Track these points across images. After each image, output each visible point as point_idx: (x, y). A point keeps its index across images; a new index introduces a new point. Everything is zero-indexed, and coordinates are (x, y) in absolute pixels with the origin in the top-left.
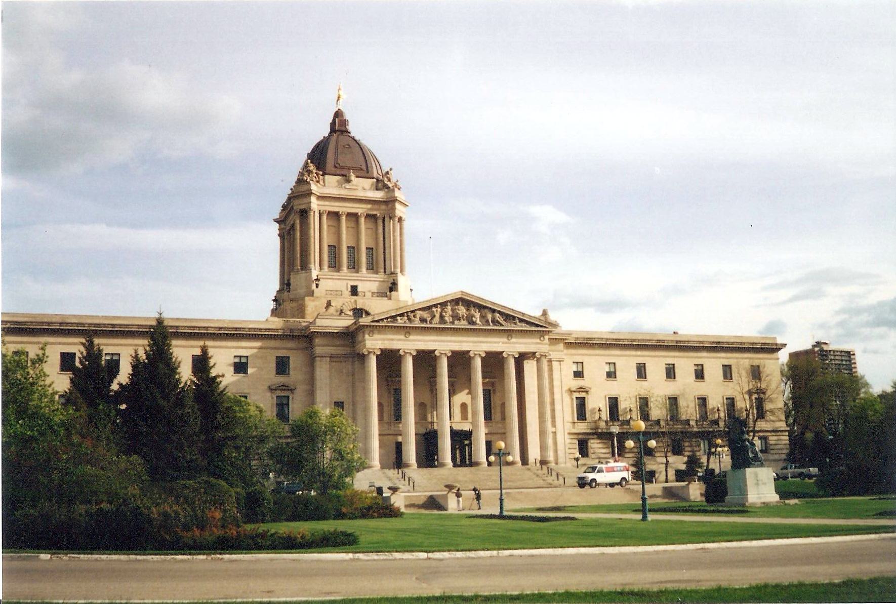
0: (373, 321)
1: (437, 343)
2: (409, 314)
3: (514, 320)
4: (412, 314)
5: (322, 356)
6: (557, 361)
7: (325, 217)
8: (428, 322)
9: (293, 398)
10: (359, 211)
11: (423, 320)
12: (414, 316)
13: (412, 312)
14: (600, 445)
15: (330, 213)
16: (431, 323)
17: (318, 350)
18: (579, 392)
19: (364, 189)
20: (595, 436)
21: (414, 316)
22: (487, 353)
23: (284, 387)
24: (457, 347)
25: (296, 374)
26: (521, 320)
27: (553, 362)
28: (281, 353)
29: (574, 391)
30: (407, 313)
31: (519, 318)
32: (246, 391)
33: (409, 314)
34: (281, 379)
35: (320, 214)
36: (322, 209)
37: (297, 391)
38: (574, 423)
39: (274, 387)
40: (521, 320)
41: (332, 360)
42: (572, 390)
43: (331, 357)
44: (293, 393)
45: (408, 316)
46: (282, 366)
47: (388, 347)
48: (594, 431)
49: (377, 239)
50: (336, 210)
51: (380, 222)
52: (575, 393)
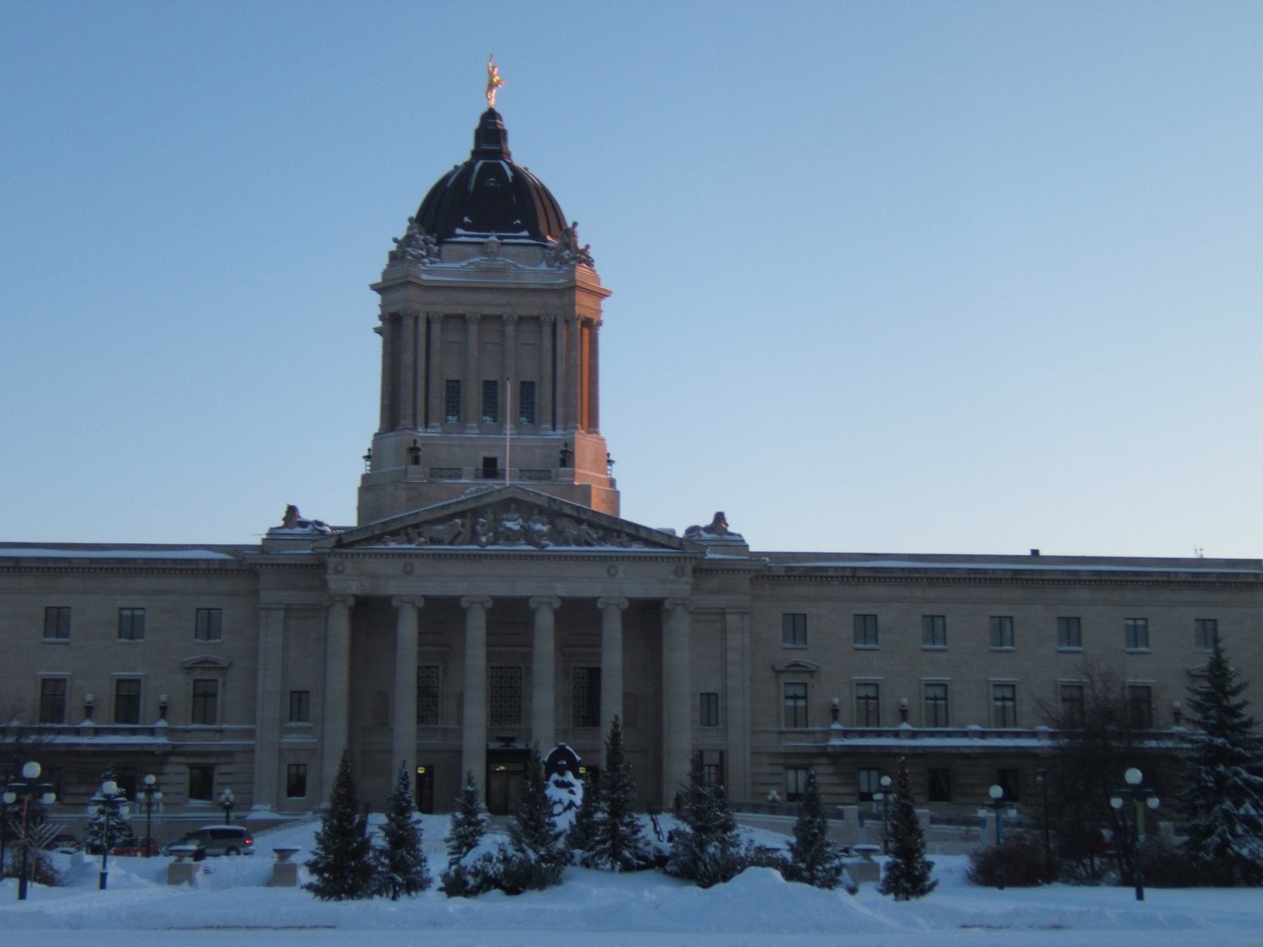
2: (409, 530)
3: (619, 537)
5: (270, 609)
7: (436, 328)
9: (224, 684)
13: (416, 526)
15: (447, 318)
17: (267, 596)
18: (794, 672)
20: (824, 761)
23: (206, 664)
27: (729, 618)
29: (781, 672)
30: (405, 528)
31: (628, 535)
33: (409, 530)
35: (428, 322)
42: (778, 669)
45: (407, 534)
46: (208, 625)
50: (460, 311)
51: (547, 330)
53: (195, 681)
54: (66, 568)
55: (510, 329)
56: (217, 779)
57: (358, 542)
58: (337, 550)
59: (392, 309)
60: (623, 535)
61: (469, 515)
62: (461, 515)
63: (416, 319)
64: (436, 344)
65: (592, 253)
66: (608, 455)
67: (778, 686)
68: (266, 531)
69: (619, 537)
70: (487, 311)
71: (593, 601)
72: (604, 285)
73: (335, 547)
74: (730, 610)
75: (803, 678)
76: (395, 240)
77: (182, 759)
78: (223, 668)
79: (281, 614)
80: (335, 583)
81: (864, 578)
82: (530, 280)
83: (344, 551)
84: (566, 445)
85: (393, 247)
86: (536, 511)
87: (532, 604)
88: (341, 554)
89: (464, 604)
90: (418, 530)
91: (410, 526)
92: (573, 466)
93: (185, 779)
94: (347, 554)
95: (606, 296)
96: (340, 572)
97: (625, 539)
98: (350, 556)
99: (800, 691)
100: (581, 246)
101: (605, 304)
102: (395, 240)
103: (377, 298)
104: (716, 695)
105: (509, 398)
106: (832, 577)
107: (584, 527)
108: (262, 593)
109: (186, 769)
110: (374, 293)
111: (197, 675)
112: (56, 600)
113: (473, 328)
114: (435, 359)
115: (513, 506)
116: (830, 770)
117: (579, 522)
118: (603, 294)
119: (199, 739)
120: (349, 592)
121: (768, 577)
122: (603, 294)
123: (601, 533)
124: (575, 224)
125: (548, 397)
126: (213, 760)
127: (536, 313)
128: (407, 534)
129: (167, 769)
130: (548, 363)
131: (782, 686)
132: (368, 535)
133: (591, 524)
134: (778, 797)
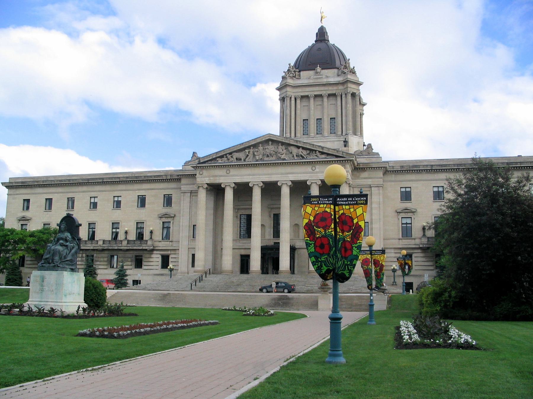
0: (199, 164)
1: (251, 177)
4: (230, 155)
5: (186, 192)
6: (376, 187)
7: (298, 101)
8: (243, 161)
10: (323, 93)
11: (238, 159)
12: (232, 157)
13: (230, 154)
14: (424, 259)
15: (302, 97)
17: (184, 188)
19: (327, 77)
20: (419, 251)
22: (292, 182)
23: (166, 215)
24: (267, 179)
26: (322, 153)
28: (167, 192)
29: (400, 212)
30: (226, 155)
31: (319, 152)
32: (143, 219)
34: (167, 210)
36: (297, 94)
38: (399, 239)
40: (322, 153)
41: (193, 194)
43: (191, 193)
44: (173, 219)
45: (227, 157)
46: (168, 201)
47: (213, 182)
48: (417, 246)
49: (337, 111)
50: (306, 94)
51: (339, 99)
52: (401, 214)
53: (163, 222)
54: (119, 181)
55: (325, 99)
56: (170, 260)
57: (207, 161)
59: (282, 96)
60: (317, 152)
61: (252, 147)
62: (249, 147)
63: (291, 98)
64: (298, 106)
65: (356, 69)
66: (364, 143)
67: (399, 219)
68: (185, 162)
69: (315, 153)
70: (316, 93)
71: (305, 182)
72: (360, 80)
74: (373, 186)
75: (409, 215)
76: (284, 72)
77: (158, 252)
78: (172, 217)
79: (189, 194)
81: (437, 170)
82: (332, 80)
84: (345, 139)
85: (284, 74)
86: (280, 144)
87: (279, 184)
88: (201, 167)
91: (227, 154)
92: (348, 147)
93: (160, 260)
94: (203, 167)
95: (362, 84)
97: (318, 154)
99: (409, 221)
100: (352, 67)
101: (361, 87)
102: (284, 72)
103: (278, 93)
104: (368, 222)
105: (326, 125)
106: (422, 170)
107: (301, 150)
108: (182, 186)
109: (160, 257)
110: (277, 91)
111: (164, 220)
113: (312, 100)
114: (298, 112)
115: (270, 143)
116: (422, 255)
117: (298, 147)
118: (359, 84)
119: (163, 245)
120: (205, 183)
121: (393, 171)
122: (359, 84)
123: (308, 152)
124: (349, 60)
125: (340, 122)
126: (169, 252)
127: (334, 92)
128: (227, 157)
129: (153, 256)
130: (340, 110)
131: (400, 219)
132: (211, 158)
133: (304, 148)
134: (396, 268)
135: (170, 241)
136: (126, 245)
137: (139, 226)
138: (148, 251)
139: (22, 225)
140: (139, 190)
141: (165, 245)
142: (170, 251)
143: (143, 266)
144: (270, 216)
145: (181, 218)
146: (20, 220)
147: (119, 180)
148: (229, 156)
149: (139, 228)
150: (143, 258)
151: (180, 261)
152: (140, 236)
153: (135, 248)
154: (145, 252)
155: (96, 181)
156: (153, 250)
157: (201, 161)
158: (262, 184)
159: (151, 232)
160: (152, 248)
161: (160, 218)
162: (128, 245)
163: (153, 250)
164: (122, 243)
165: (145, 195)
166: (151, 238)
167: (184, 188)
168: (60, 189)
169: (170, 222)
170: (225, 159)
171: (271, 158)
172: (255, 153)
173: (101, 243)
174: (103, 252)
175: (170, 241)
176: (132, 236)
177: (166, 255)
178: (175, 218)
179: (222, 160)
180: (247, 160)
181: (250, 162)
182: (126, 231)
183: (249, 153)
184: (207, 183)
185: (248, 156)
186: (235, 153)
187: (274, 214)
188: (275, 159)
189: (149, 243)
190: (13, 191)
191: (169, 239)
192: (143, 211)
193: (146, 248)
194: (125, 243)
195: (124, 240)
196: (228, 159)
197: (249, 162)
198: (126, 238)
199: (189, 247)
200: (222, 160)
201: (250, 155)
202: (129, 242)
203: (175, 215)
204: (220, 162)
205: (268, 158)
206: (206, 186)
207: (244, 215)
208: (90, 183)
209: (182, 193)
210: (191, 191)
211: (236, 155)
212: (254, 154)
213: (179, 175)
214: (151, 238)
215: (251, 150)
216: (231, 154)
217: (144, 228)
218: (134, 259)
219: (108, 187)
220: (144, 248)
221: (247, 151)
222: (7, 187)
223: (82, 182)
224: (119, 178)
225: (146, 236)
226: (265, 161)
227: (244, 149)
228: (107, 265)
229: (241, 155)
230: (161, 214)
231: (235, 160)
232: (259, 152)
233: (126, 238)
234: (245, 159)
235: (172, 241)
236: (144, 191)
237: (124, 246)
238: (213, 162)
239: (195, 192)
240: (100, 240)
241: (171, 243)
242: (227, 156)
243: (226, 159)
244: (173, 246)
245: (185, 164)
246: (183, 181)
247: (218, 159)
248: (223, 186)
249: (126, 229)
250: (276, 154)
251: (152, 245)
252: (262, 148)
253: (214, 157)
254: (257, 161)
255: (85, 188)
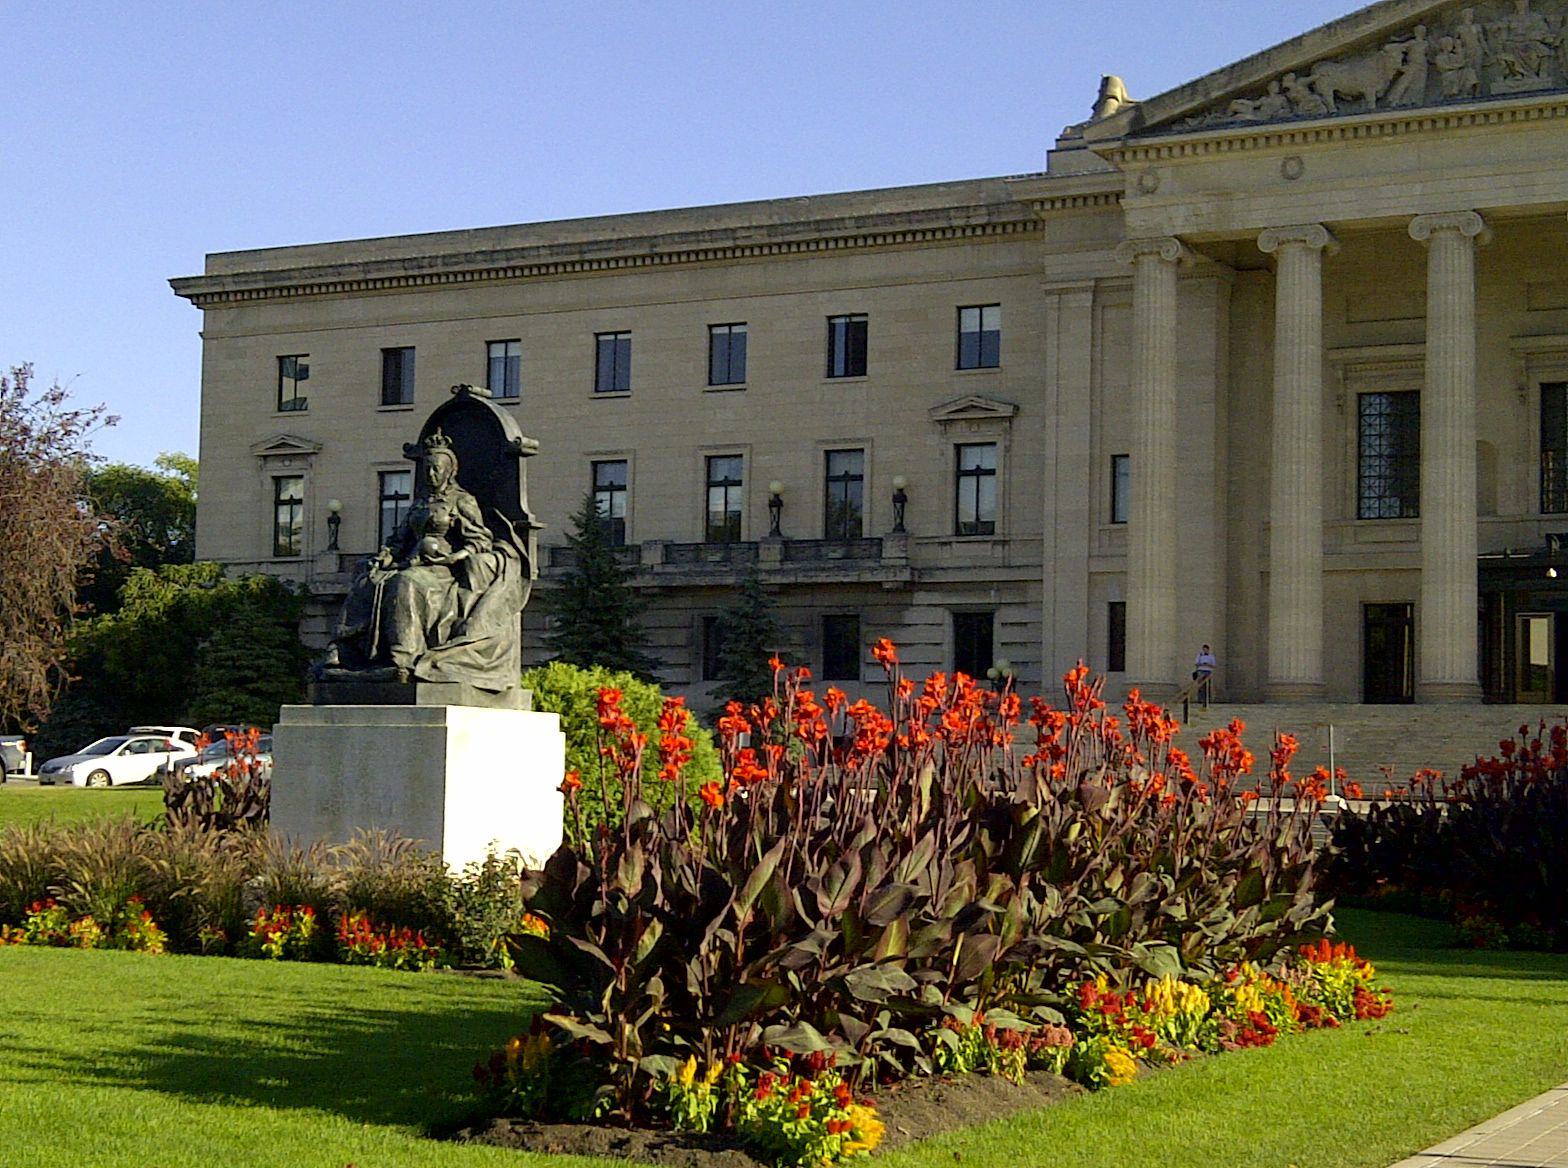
2: (1289, 81)
9: (1008, 449)
11: (1347, 101)
12: (1311, 88)
13: (1304, 71)
16: (1382, 102)
21: (1311, 88)
23: (968, 412)
25: (1012, 371)
30: (1279, 77)
34: (971, 384)
37: (1021, 423)
39: (942, 415)
43: (1096, 292)
45: (1284, 91)
53: (958, 447)
56: (999, 635)
57: (1181, 119)
58: (1132, 142)
61: (1420, 29)
62: (1405, 31)
73: (1133, 134)
79: (1086, 299)
80: (1138, 215)
83: (1147, 141)
89: (1415, 234)
90: (1308, 80)
91: (1287, 72)
93: (946, 634)
96: (1152, 191)
98: (1164, 153)
108: (1049, 260)
109: (948, 620)
112: (721, 311)
120: (1168, 232)
128: (1284, 91)
129: (911, 616)
132: (1195, 104)
135: (995, 543)
136: (778, 565)
137: (840, 467)
138: (888, 591)
139: (277, 480)
140: (833, 288)
141: (968, 563)
142: (998, 590)
143: (863, 668)
144: (1523, 399)
145: (1051, 420)
146: (265, 457)
147: (730, 243)
148: (1297, 86)
149: (838, 479)
150: (864, 629)
151: (1047, 636)
152: (843, 522)
153: (822, 578)
154: (870, 598)
155: (621, 253)
156: (910, 587)
157: (1149, 122)
158: (1478, 227)
159: (900, 498)
160: (905, 576)
161: (940, 428)
162: (789, 565)
163: (910, 587)
164: (757, 556)
165: (866, 315)
166: (900, 528)
167: (1057, 265)
168: (446, 301)
169: (993, 444)
170: (1273, 101)
171: (1533, 83)
172: (1441, 60)
173: (652, 558)
174: (669, 603)
175: (995, 543)
176: (805, 522)
177: (973, 610)
178: (1016, 422)
179: (1257, 108)
180: (1394, 98)
181: (1414, 106)
182: (777, 496)
183: (1405, 61)
184: (1178, 233)
185: (1400, 74)
186: (1328, 69)
187: (1546, 388)
188: (1550, 85)
189: (891, 550)
190: (226, 316)
191: (992, 533)
192: (852, 390)
193: (879, 577)
194: (771, 556)
195: (765, 541)
196: (1292, 103)
197: (1403, 107)
198: (776, 531)
199: (1093, 570)
200: (1257, 108)
201: (1410, 71)
202: (791, 549)
203: (1017, 408)
204: (1249, 117)
205: (1509, 82)
206: (1175, 251)
207: (1380, 394)
208: (591, 262)
209: (1049, 293)
210: (1097, 280)
211: (1331, 78)
212: (1431, 64)
213: (1033, 202)
214: (900, 528)
215: (1419, 47)
216: (1308, 75)
217: (860, 478)
218: (818, 631)
219: (678, 282)
220: (868, 577)
221: (1394, 51)
222: (198, 300)
223: (551, 260)
224: (734, 230)
225: (876, 518)
226: (1504, 96)
227: (1381, 40)
228: (688, 665)
229: (1367, 77)
230: (944, 406)
231: (1331, 100)
232: (1459, 50)
233: (776, 531)
234: (1387, 92)
235: (1004, 543)
236: (857, 294)
237: (769, 572)
238: (1209, 120)
239: (1119, 289)
240: (648, 543)
241: (1000, 548)
242: (1286, 84)
243: (1279, 100)
244: (1010, 567)
245: (1063, 144)
246: (1053, 232)
247: (1235, 105)
248: (1265, 246)
249: (776, 487)
250: (1557, 57)
251: (904, 562)
252: (1475, 29)
253: (1215, 94)
254: (1451, 100)
255: (565, 290)
